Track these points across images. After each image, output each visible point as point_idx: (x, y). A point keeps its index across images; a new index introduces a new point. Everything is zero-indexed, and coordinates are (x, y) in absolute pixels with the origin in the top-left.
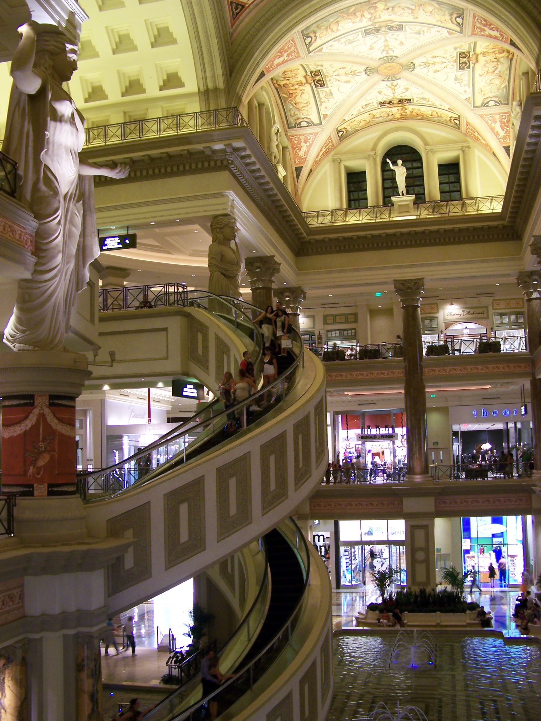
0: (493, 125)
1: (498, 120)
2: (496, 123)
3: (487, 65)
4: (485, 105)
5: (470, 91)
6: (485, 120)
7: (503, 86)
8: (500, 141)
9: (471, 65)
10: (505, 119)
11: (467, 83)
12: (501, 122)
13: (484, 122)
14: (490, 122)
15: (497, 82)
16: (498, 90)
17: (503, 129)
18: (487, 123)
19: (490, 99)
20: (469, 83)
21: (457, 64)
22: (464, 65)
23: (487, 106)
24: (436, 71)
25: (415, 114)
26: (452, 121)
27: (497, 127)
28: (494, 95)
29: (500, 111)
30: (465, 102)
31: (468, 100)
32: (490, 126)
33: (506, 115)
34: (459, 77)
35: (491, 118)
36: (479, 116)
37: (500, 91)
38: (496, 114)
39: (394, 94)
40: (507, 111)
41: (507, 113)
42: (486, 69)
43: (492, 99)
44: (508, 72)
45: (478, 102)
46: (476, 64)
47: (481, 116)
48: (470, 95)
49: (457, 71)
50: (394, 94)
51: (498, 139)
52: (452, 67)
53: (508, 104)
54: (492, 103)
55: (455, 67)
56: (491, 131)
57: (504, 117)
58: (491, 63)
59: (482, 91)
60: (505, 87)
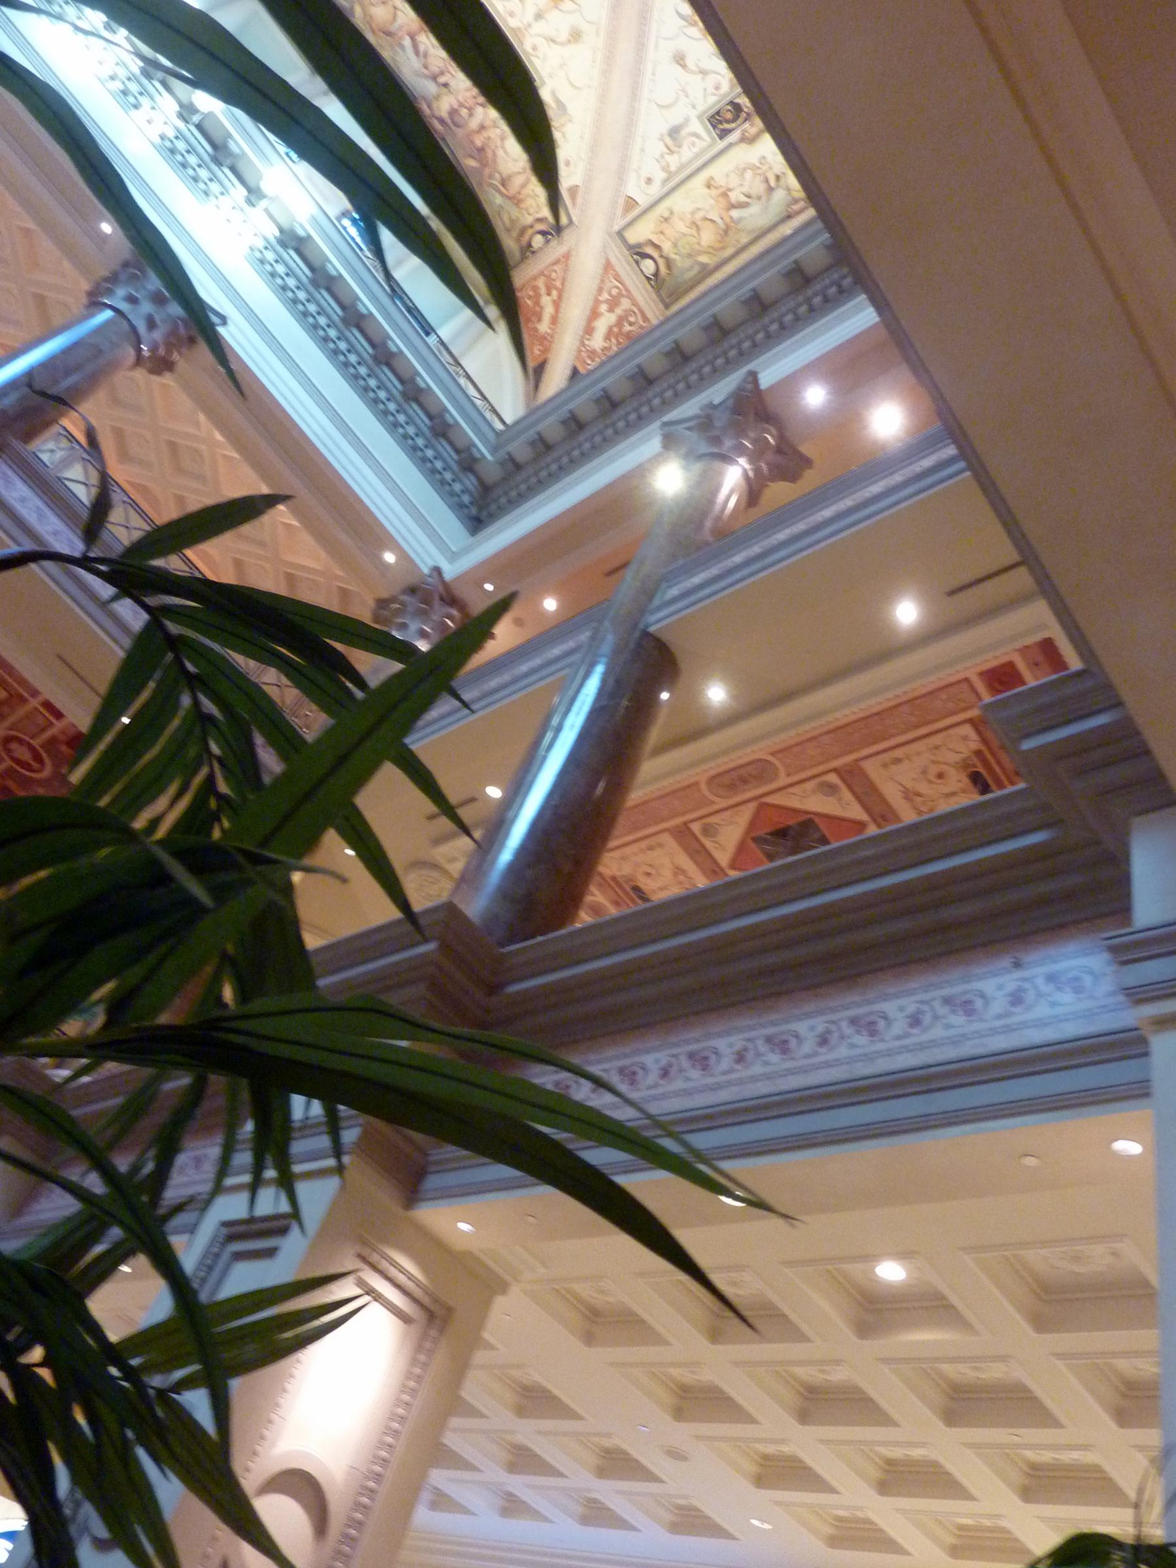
0: (603, 308)
1: (619, 311)
2: (611, 310)
3: (749, 174)
4: (639, 253)
5: (655, 190)
6: (602, 281)
7: (704, 259)
8: (580, 351)
9: (734, 137)
10: (631, 324)
11: (673, 168)
12: (620, 322)
13: (597, 282)
14: (605, 296)
15: (708, 237)
16: (689, 256)
17: (607, 337)
18: (600, 290)
19: (655, 254)
20: (682, 167)
21: (725, 96)
22: (729, 116)
23: (637, 262)
24: (680, 59)
25: (479, 143)
26: (530, 231)
27: (606, 320)
28: (673, 256)
29: (642, 303)
30: (621, 201)
31: (631, 203)
32: (597, 302)
33: (641, 322)
34: (684, 133)
35: (614, 292)
36: (603, 261)
37: (688, 263)
38: (630, 296)
39: (539, 16)
40: (650, 315)
41: (645, 319)
42: (734, 181)
43: (661, 261)
44: (745, 240)
45: (636, 235)
46: (743, 145)
47: (608, 266)
48: (643, 201)
49: (700, 117)
50: (539, 16)
51: (583, 344)
52: (711, 90)
53: (667, 306)
54: (648, 266)
55: (712, 100)
56: (588, 312)
57: (632, 319)
58: (758, 179)
59: (666, 220)
60: (704, 266)
